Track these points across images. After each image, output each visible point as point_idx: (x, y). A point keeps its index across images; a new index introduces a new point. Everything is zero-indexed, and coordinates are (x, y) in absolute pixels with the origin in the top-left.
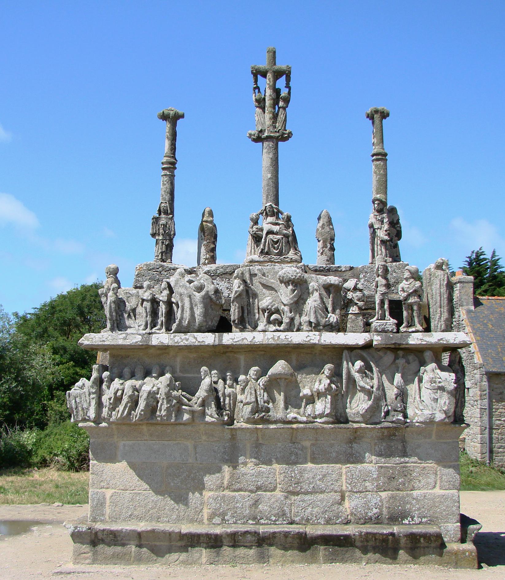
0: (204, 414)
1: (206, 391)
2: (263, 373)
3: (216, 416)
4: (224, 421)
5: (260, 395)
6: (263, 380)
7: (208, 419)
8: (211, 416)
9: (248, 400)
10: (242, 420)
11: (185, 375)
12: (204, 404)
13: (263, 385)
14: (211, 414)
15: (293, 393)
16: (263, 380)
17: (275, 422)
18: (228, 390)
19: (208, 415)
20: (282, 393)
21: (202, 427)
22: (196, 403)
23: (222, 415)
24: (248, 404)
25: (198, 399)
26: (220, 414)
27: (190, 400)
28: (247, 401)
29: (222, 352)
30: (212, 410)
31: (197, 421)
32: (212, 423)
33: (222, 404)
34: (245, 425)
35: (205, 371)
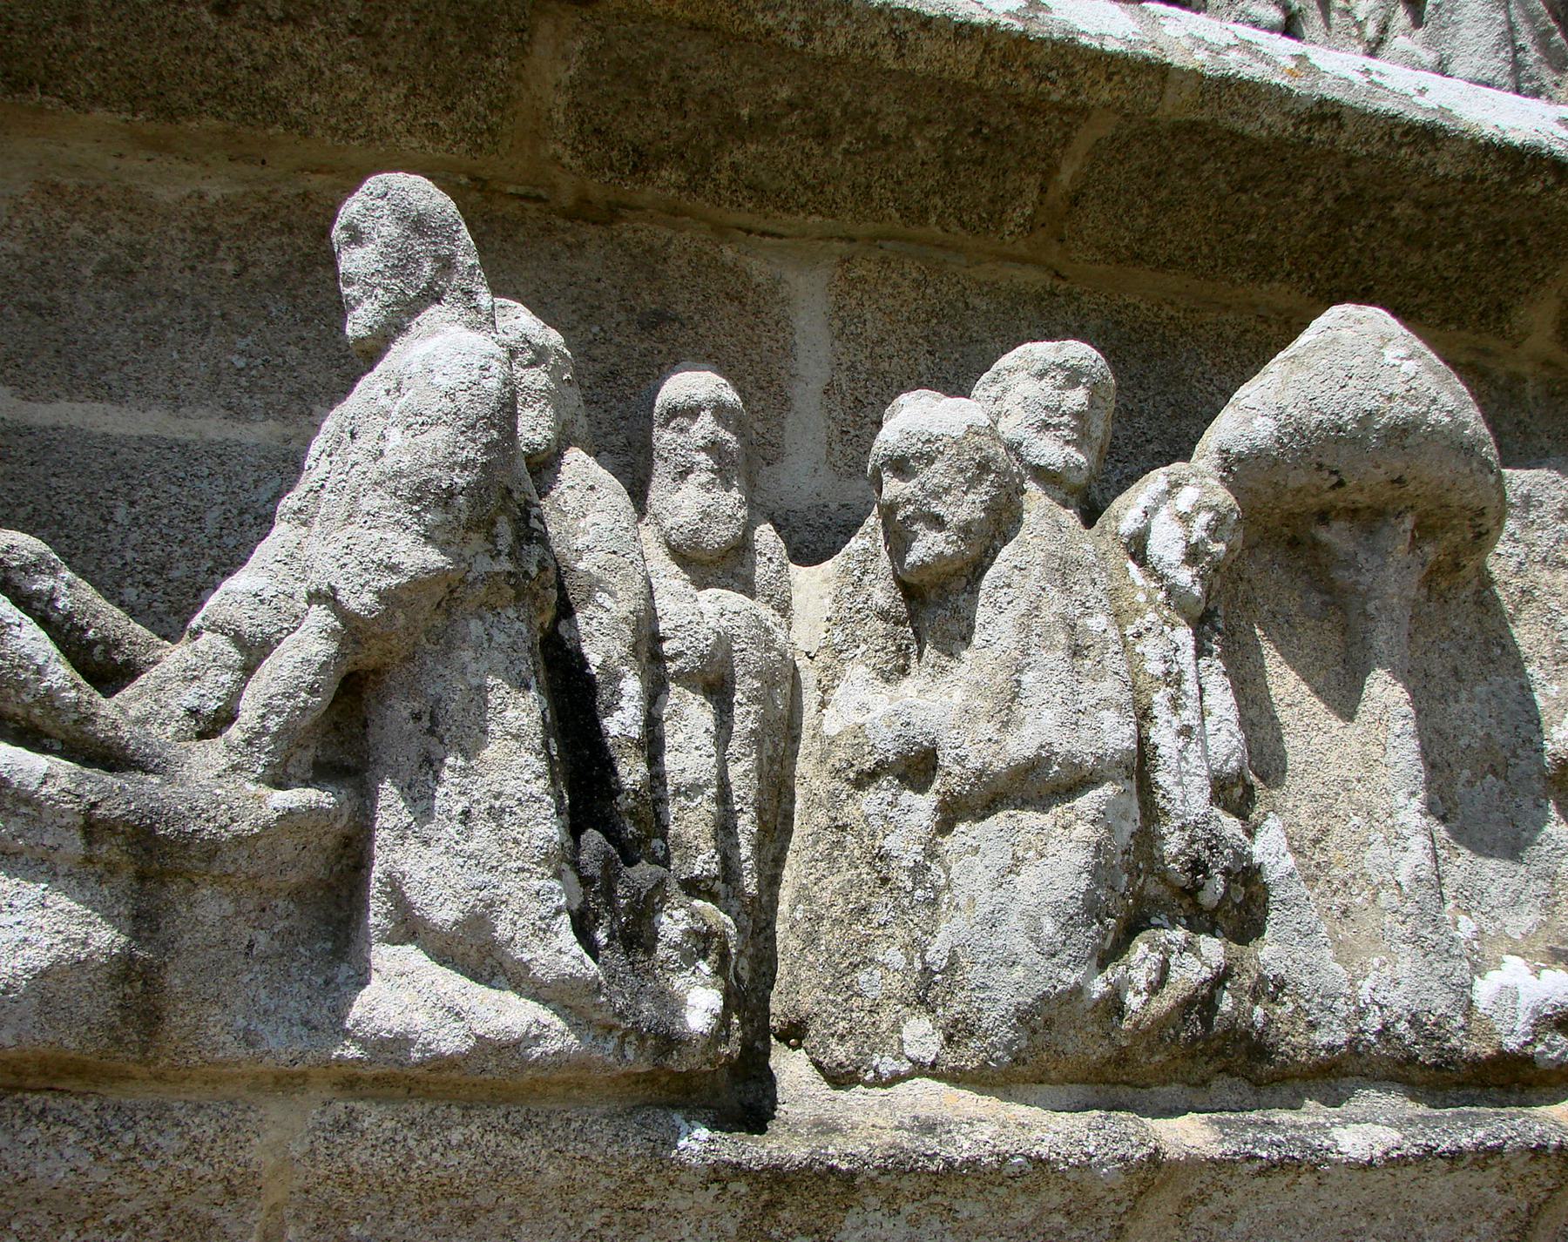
0: (332, 902)
1: (426, 496)
2: (1144, 426)
3: (561, 953)
4: (669, 1041)
5: (1174, 680)
6: (1176, 507)
7: (405, 997)
8: (476, 952)
9: (1038, 731)
10: (921, 1036)
11: (43, 414)
12: (360, 722)
13: (1193, 555)
14: (478, 922)
15: (1470, 713)
16: (1176, 507)
17: (1335, 1075)
18: (695, 613)
19: (409, 927)
20: (1385, 692)
21: (280, 1137)
22: (221, 720)
23: (637, 937)
24: (1037, 784)
25: (254, 652)
26: (614, 915)
27: (107, 670)
28: (1021, 745)
29: (567, 199)
30: (473, 834)
31: (225, 1020)
32: (481, 1080)
33: (631, 772)
34: (985, 1125)
35: (418, 225)
